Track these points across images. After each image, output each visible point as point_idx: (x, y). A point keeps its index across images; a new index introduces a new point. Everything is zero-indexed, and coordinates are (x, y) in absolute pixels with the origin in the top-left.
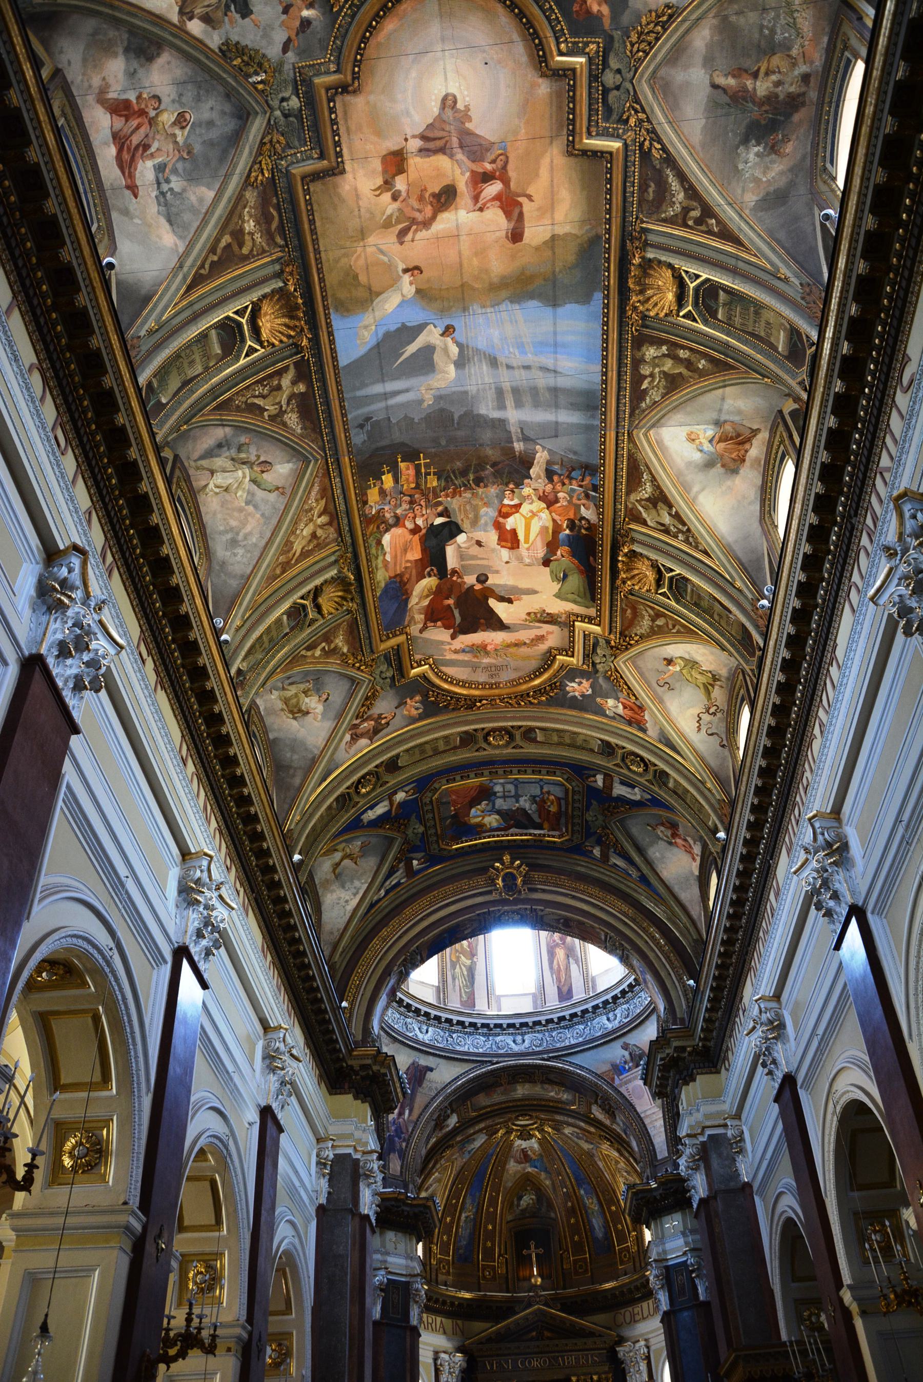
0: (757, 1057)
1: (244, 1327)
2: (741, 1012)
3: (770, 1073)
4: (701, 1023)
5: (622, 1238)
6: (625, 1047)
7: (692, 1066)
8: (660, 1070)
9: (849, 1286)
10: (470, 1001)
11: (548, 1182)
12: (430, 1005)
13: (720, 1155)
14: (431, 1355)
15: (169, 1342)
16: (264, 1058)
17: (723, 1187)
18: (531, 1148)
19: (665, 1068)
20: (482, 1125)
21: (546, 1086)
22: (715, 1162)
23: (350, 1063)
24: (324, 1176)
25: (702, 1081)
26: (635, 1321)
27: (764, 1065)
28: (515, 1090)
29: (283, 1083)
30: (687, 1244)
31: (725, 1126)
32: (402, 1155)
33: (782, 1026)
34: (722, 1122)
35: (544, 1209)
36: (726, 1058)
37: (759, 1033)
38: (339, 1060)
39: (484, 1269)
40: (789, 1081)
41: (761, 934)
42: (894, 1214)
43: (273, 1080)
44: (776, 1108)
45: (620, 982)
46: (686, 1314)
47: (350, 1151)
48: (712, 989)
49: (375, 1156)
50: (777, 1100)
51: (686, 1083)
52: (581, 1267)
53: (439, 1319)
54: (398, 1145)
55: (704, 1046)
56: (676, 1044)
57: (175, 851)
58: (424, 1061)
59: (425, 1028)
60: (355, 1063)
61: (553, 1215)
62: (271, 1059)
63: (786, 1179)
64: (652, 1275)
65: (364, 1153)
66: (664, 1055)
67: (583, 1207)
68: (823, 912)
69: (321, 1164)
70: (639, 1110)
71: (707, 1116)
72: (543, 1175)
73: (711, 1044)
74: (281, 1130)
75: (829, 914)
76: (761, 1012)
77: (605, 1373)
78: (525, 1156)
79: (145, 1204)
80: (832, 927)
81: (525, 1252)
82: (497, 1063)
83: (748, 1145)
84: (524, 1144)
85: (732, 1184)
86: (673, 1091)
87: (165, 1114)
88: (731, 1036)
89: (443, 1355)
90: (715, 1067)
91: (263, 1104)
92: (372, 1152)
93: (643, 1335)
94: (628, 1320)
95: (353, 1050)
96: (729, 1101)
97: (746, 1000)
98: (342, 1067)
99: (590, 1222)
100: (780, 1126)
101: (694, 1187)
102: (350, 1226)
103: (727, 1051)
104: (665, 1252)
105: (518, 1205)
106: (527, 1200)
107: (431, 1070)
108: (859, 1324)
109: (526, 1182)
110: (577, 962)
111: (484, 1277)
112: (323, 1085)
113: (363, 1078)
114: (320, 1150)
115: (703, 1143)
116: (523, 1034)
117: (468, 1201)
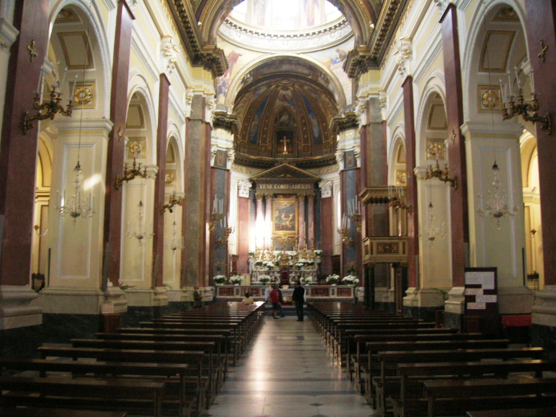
0: (397, 66)
1: (156, 168)
2: (393, 43)
3: (402, 74)
4: (374, 46)
5: (327, 138)
6: (338, 51)
7: (367, 65)
8: (352, 66)
9: (419, 168)
10: (262, 23)
11: (294, 111)
12: (242, 23)
13: (374, 107)
15: (126, 173)
16: (161, 51)
17: (373, 121)
18: (288, 95)
19: (354, 65)
20: (265, 82)
21: (297, 66)
22: (372, 110)
23: (202, 52)
24: (189, 104)
25: (371, 73)
27: (400, 69)
28: (282, 67)
29: (170, 62)
30: (355, 143)
31: (379, 94)
32: (225, 95)
33: (411, 53)
34: (377, 92)
35: (291, 123)
36: (384, 63)
37: (400, 54)
38: (196, 51)
39: (262, 146)
40: (409, 79)
41: (408, 7)
42: (442, 141)
43: (166, 61)
44: (402, 90)
45: (339, 19)
46: (350, 172)
47: (201, 93)
48: (382, 30)
49: (213, 96)
50: (403, 86)
51: (363, 72)
52: (306, 149)
54: (223, 91)
55: (374, 57)
56: (361, 54)
57: (159, 36)
58: (238, 51)
59: (238, 34)
60: (205, 53)
61: (295, 125)
62: (164, 51)
63: (401, 121)
64: (338, 155)
65: (208, 95)
66: (354, 59)
67: (310, 124)
68: (437, 4)
69: (188, 99)
70: (341, 81)
71: (371, 89)
72: (292, 107)
73: (378, 56)
74: (169, 84)
75: (440, 5)
76: (402, 45)
78: (284, 98)
79: (113, 117)
80: (440, 11)
81: (281, 141)
82: (274, 54)
83: (388, 104)
84: (284, 92)
85: (378, 121)
86: (357, 76)
87: (118, 79)
88: (387, 54)
90: (378, 66)
91: (161, 72)
92: (211, 94)
95: (203, 46)
96: (382, 84)
97: (396, 38)
98: (198, 54)
100: (402, 99)
101: (360, 120)
102: (202, 127)
103: (385, 60)
104: (345, 146)
105: (280, 120)
106: (284, 118)
107: (241, 55)
108: (419, 183)
109: (284, 110)
110: (318, 6)
112: (189, 63)
113: (208, 60)
114: (187, 92)
115: (368, 102)
116: (288, 41)
117: (256, 117)
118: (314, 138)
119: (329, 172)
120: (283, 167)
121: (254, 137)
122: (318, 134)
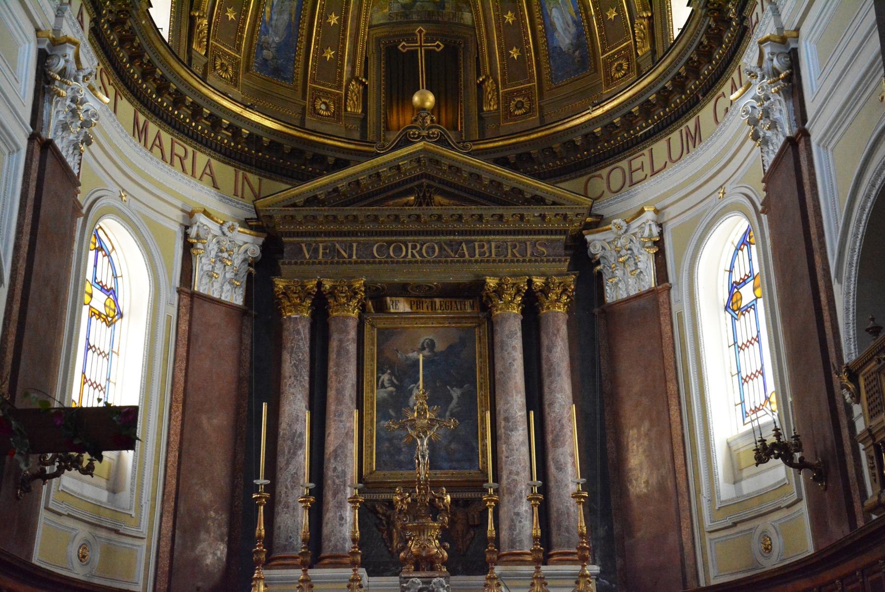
14: (177, 215)
26: (632, 184)
39: (317, 95)
53: (202, 159)
61: (467, 17)
77: (560, 274)
89: (202, 219)
93: (648, 203)
94: (615, 186)
99: (545, 16)
111: (315, 112)
118: (555, 52)
119: (637, 176)
120: (416, 158)
121: (280, 48)
122: (573, 29)
